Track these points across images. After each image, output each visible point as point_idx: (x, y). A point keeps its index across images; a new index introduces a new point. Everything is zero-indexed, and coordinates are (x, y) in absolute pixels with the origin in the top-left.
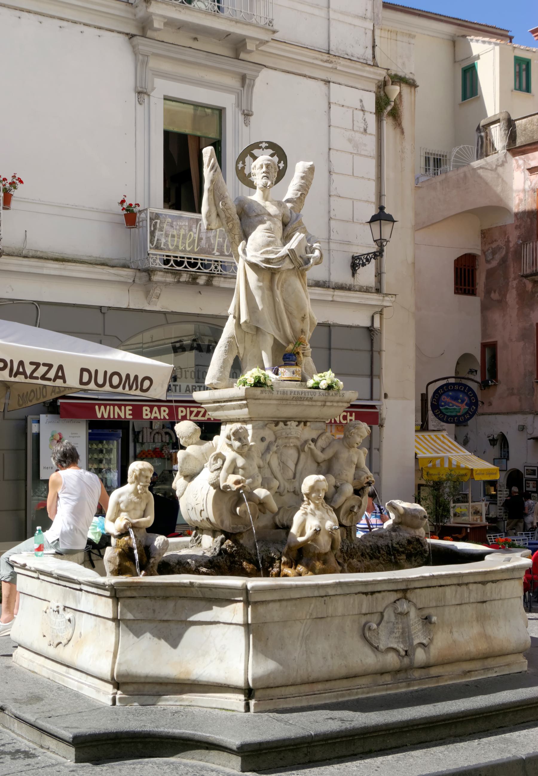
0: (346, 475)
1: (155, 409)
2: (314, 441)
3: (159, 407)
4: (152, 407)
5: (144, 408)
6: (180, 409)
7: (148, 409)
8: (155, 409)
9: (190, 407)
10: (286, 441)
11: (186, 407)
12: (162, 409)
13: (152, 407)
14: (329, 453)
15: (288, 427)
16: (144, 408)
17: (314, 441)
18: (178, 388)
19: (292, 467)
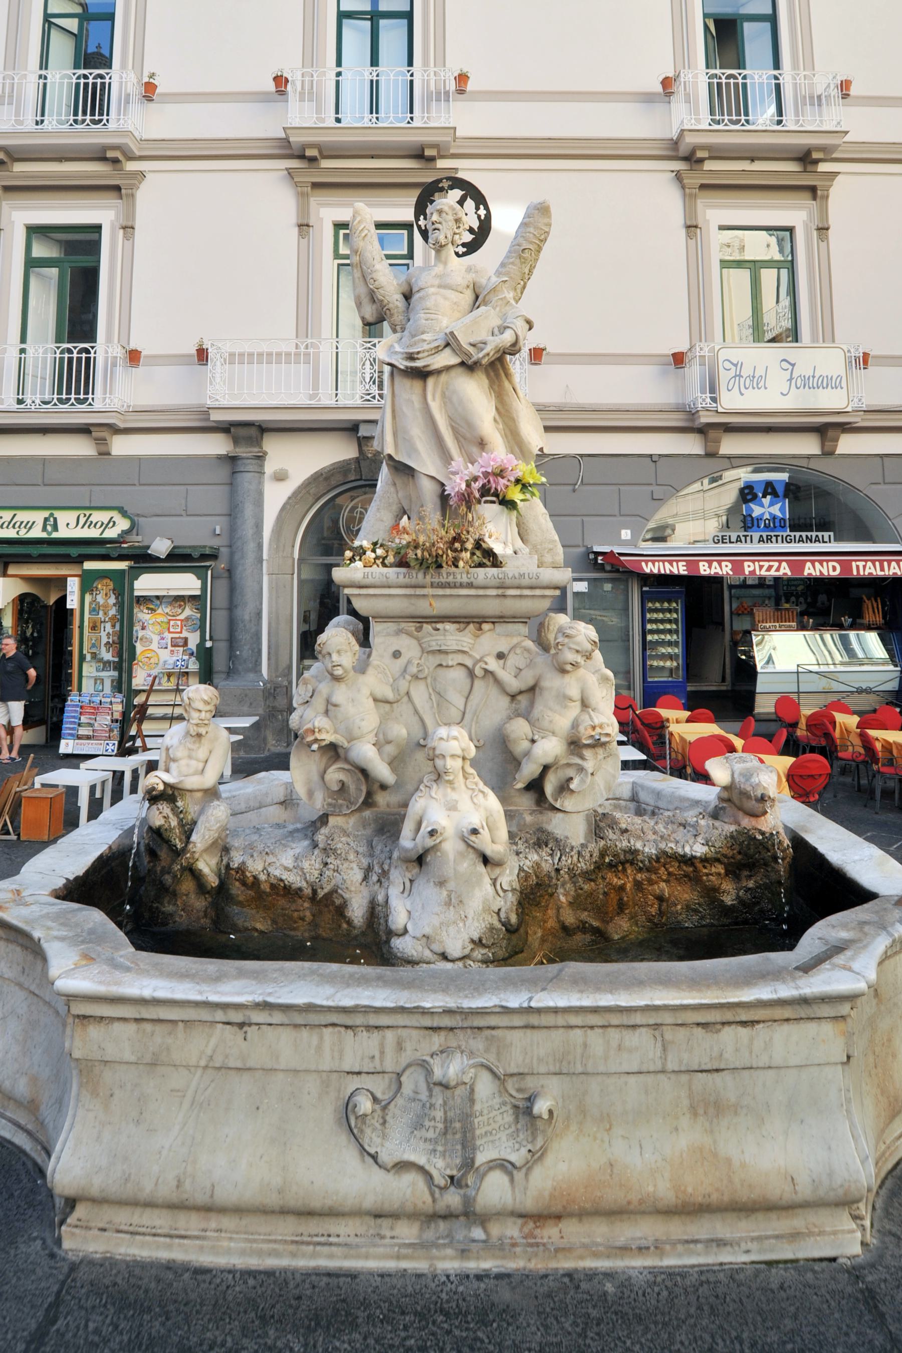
0: (551, 722)
1: (715, 564)
2: (501, 656)
3: (719, 562)
4: (710, 563)
5: (701, 564)
6: (746, 564)
7: (706, 564)
8: (715, 564)
9: (759, 561)
10: (442, 656)
11: (753, 561)
12: (724, 564)
13: (710, 563)
14: (528, 679)
15: (441, 632)
16: (701, 564)
17: (501, 656)
18: (748, 539)
19: (459, 702)
